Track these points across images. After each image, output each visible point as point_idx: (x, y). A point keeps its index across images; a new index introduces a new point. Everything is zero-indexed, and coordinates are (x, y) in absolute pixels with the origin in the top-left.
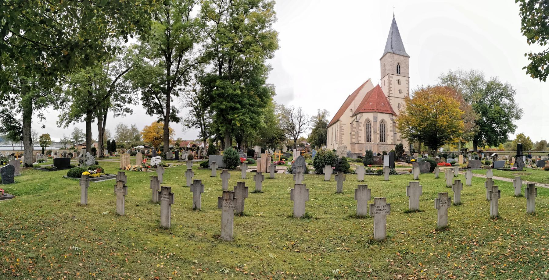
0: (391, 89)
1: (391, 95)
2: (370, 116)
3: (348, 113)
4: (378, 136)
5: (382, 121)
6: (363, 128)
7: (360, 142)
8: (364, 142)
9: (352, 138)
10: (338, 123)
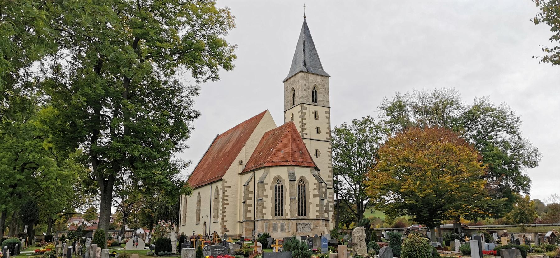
0: (305, 127)
1: (305, 136)
2: (283, 173)
3: (235, 167)
4: (296, 205)
5: (302, 179)
6: (270, 192)
7: (265, 218)
8: (271, 218)
9: (246, 211)
10: (219, 184)
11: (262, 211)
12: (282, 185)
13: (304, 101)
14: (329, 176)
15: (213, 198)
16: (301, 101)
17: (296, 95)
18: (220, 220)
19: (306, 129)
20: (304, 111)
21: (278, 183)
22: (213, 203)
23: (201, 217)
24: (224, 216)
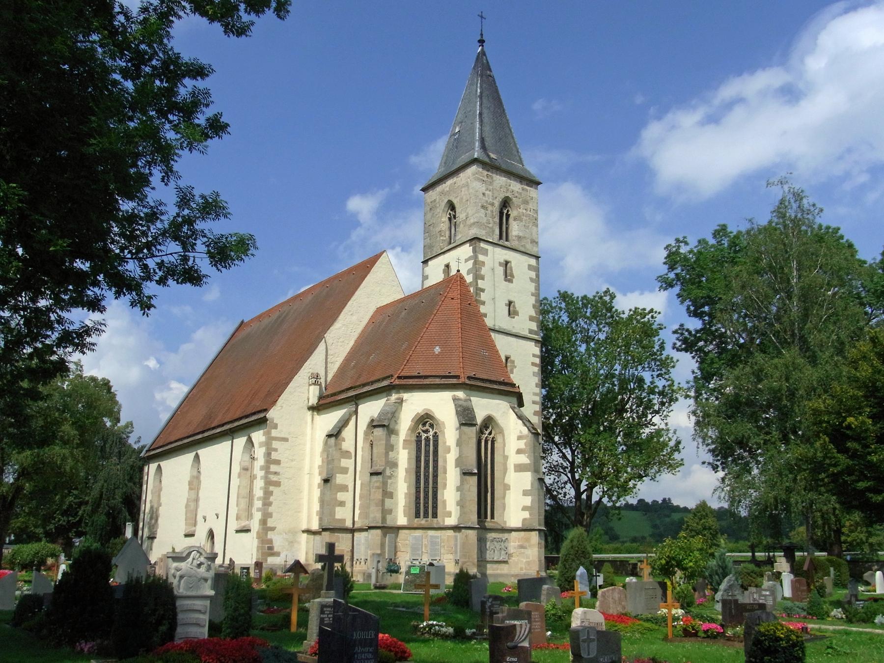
3: (301, 391)
6: (404, 457)
7: (389, 523)
8: (402, 520)
11: (383, 502)
12: (436, 436)
13: (482, 234)
15: (236, 469)
16: (473, 232)
17: (461, 215)
18: (255, 525)
20: (481, 258)
21: (426, 431)
22: (235, 481)
23: (200, 518)
24: (266, 516)
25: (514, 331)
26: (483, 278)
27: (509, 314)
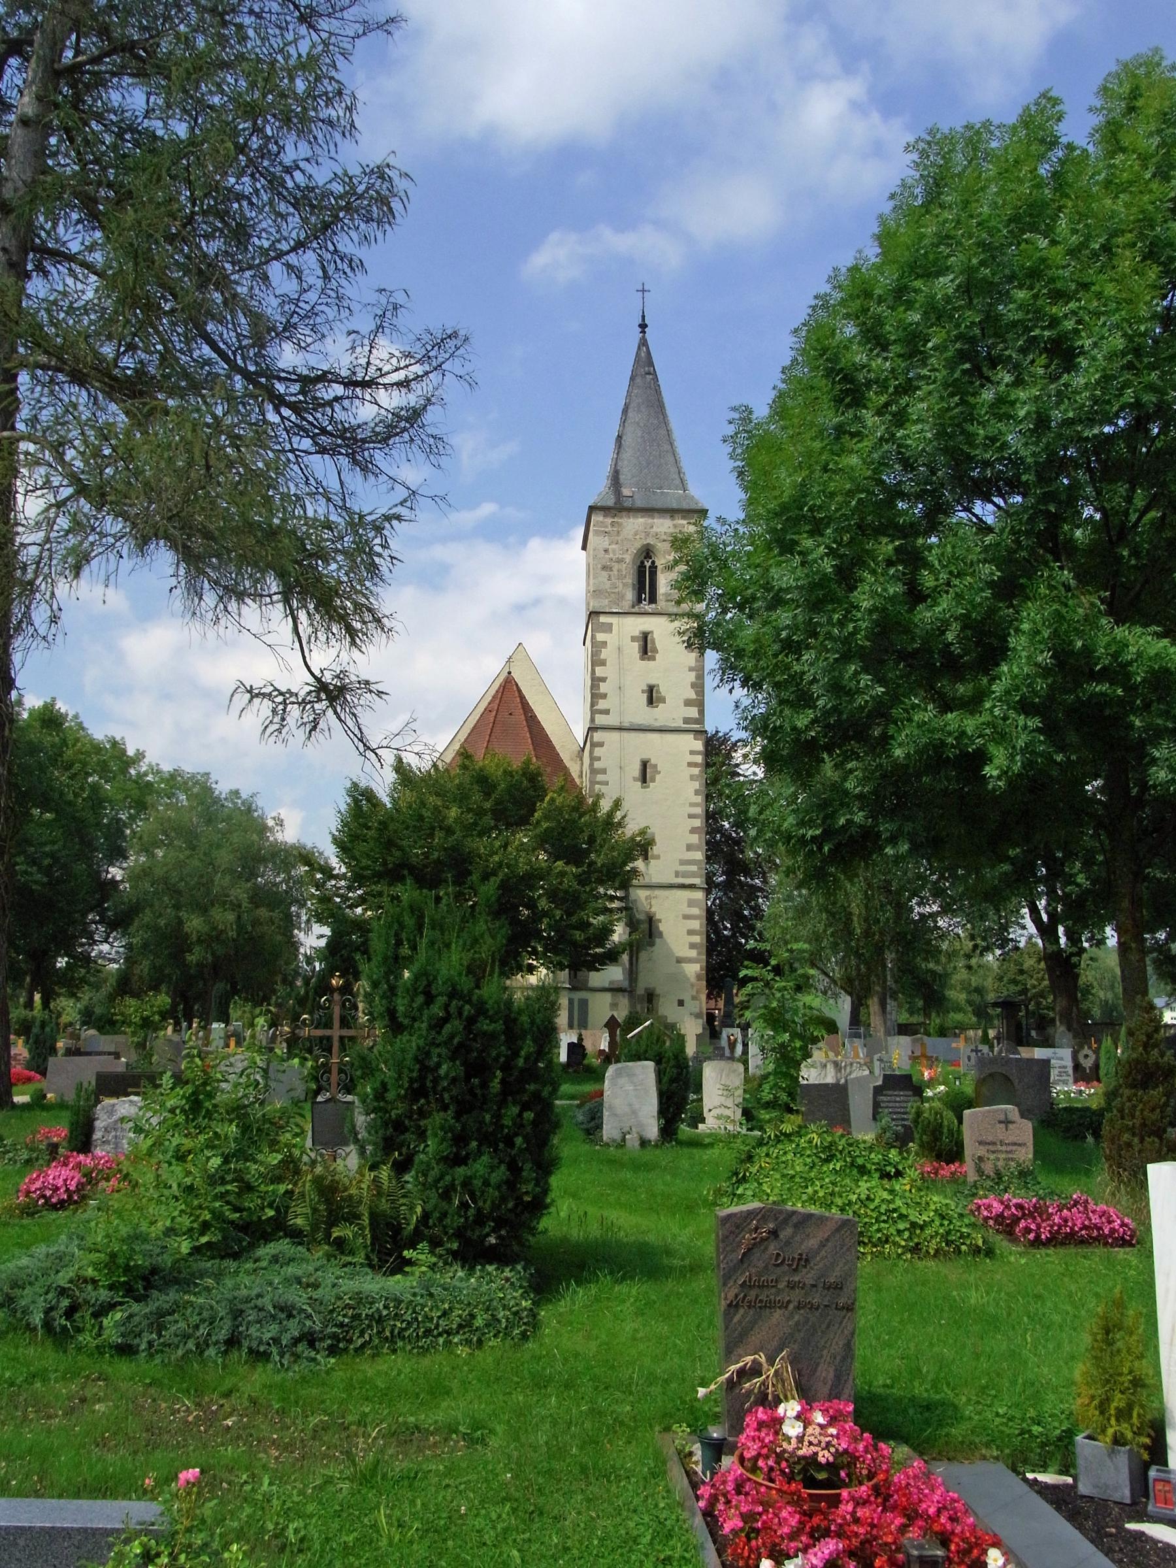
0: (603, 688)
14: (689, 848)
19: (604, 696)
20: (600, 637)
25: (657, 724)
26: (603, 663)
27: (650, 701)
